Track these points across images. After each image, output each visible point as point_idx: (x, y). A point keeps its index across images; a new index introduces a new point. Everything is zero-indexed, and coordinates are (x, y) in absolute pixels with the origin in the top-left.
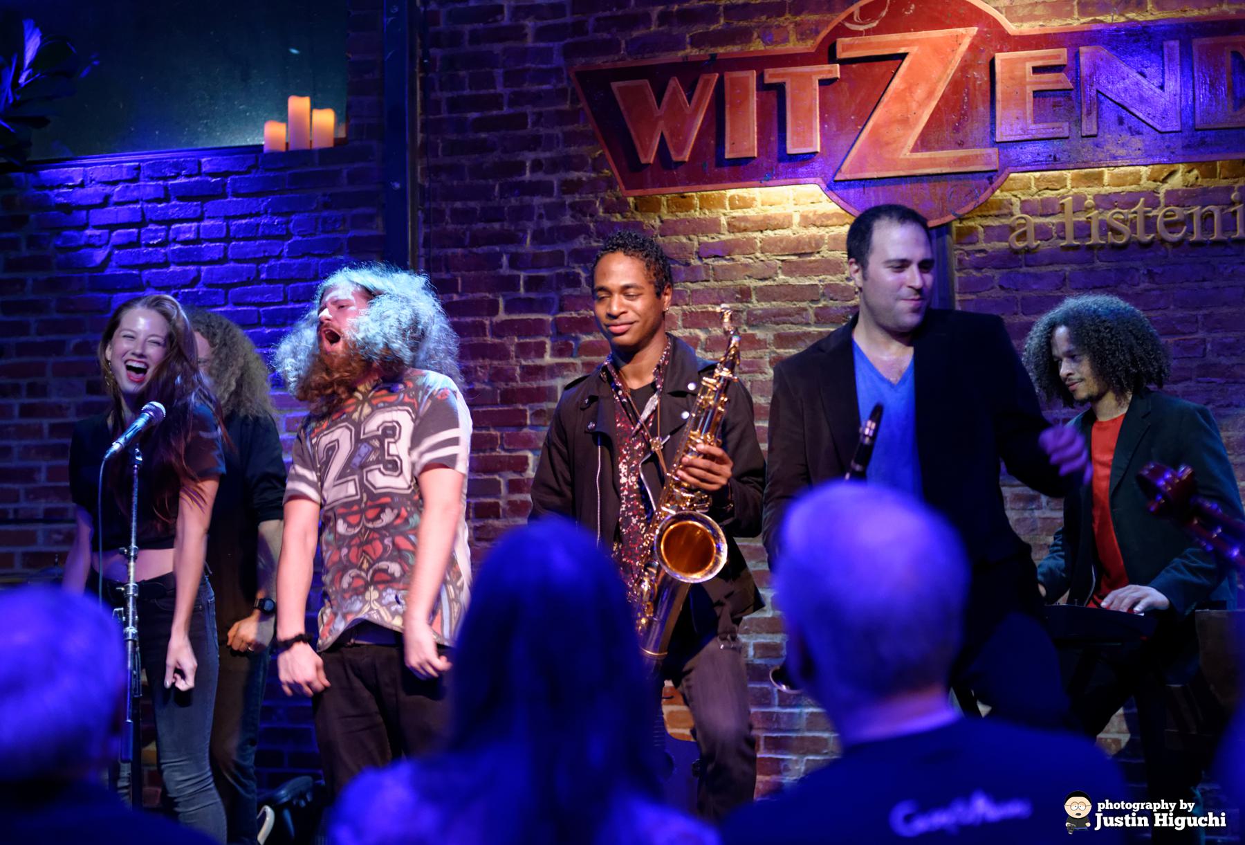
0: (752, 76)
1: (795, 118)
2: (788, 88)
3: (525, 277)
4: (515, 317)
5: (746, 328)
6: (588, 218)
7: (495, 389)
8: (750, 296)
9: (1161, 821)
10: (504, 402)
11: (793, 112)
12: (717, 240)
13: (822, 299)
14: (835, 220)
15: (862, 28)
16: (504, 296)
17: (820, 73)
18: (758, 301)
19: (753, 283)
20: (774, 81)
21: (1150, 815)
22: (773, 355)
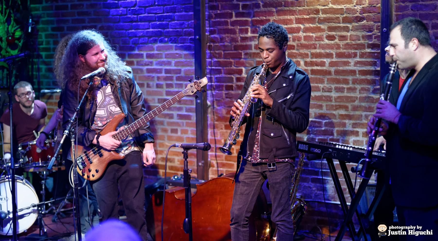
3: (242, 4)
4: (238, 19)
5: (317, 24)
7: (232, 45)
8: (319, 12)
9: (411, 233)
10: (235, 49)
13: (345, 14)
16: (235, 11)
18: (322, 14)
21: (407, 230)
22: (327, 34)
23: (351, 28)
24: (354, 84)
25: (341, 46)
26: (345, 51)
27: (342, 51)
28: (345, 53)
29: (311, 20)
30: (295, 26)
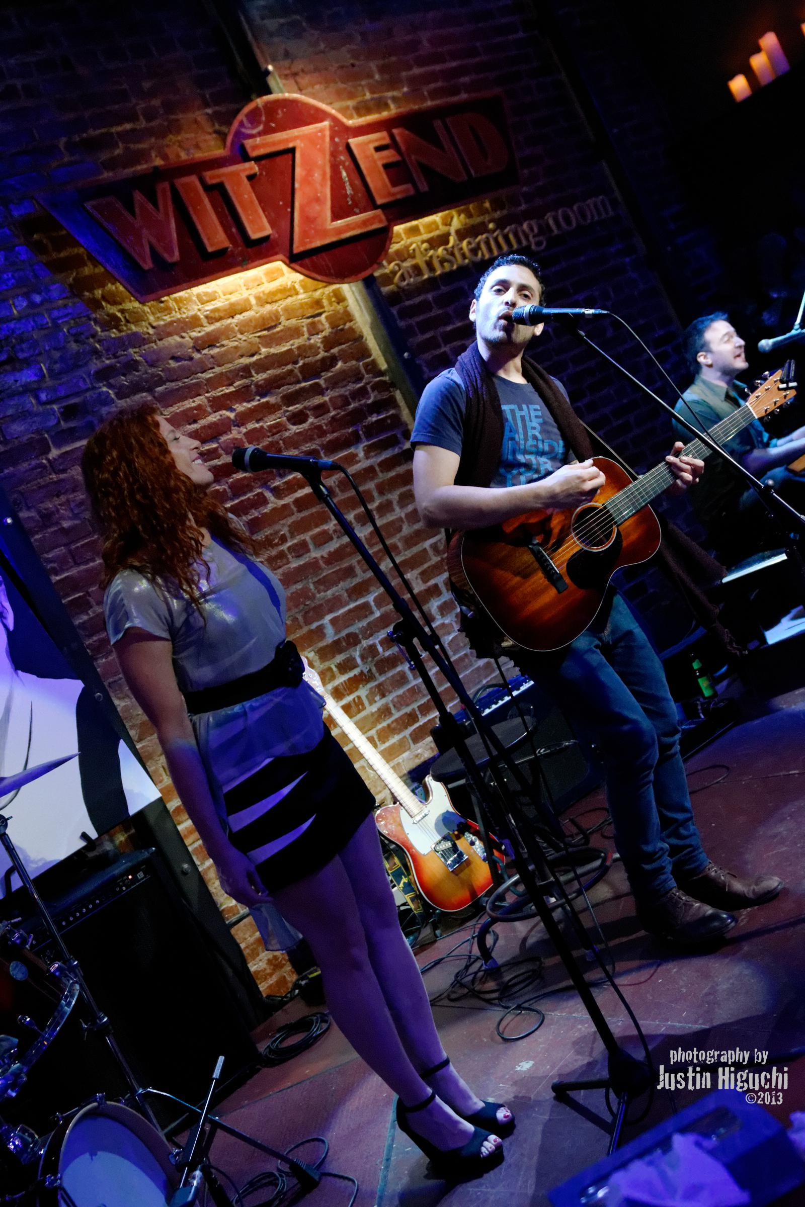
0: (193, 179)
1: (244, 209)
2: (228, 187)
6: (91, 340)
8: (250, 372)
11: (241, 203)
12: (203, 333)
14: (279, 296)
15: (254, 131)
17: (244, 170)
19: (246, 361)
20: (214, 181)
22: (287, 414)
23: (324, 386)
24: (384, 494)
25: (324, 427)
26: (335, 435)
27: (329, 437)
28: (337, 439)
29: (243, 394)
30: (213, 418)
